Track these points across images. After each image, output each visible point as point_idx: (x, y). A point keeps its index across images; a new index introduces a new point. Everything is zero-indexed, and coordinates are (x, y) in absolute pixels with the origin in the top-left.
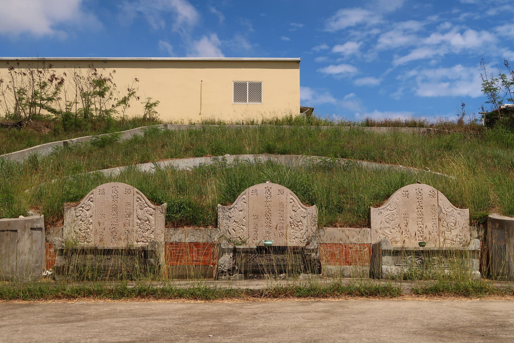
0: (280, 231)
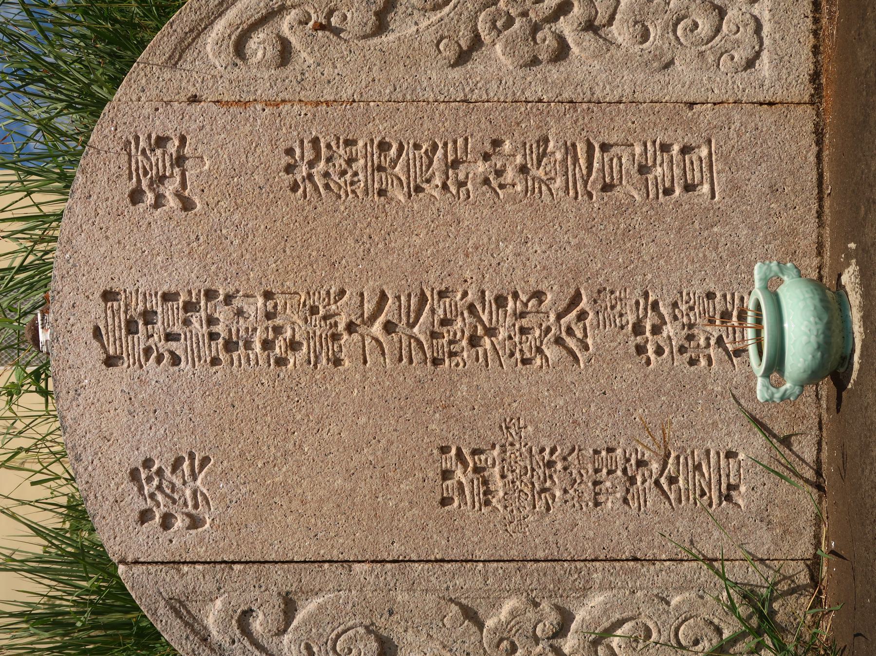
0: (629, 189)
